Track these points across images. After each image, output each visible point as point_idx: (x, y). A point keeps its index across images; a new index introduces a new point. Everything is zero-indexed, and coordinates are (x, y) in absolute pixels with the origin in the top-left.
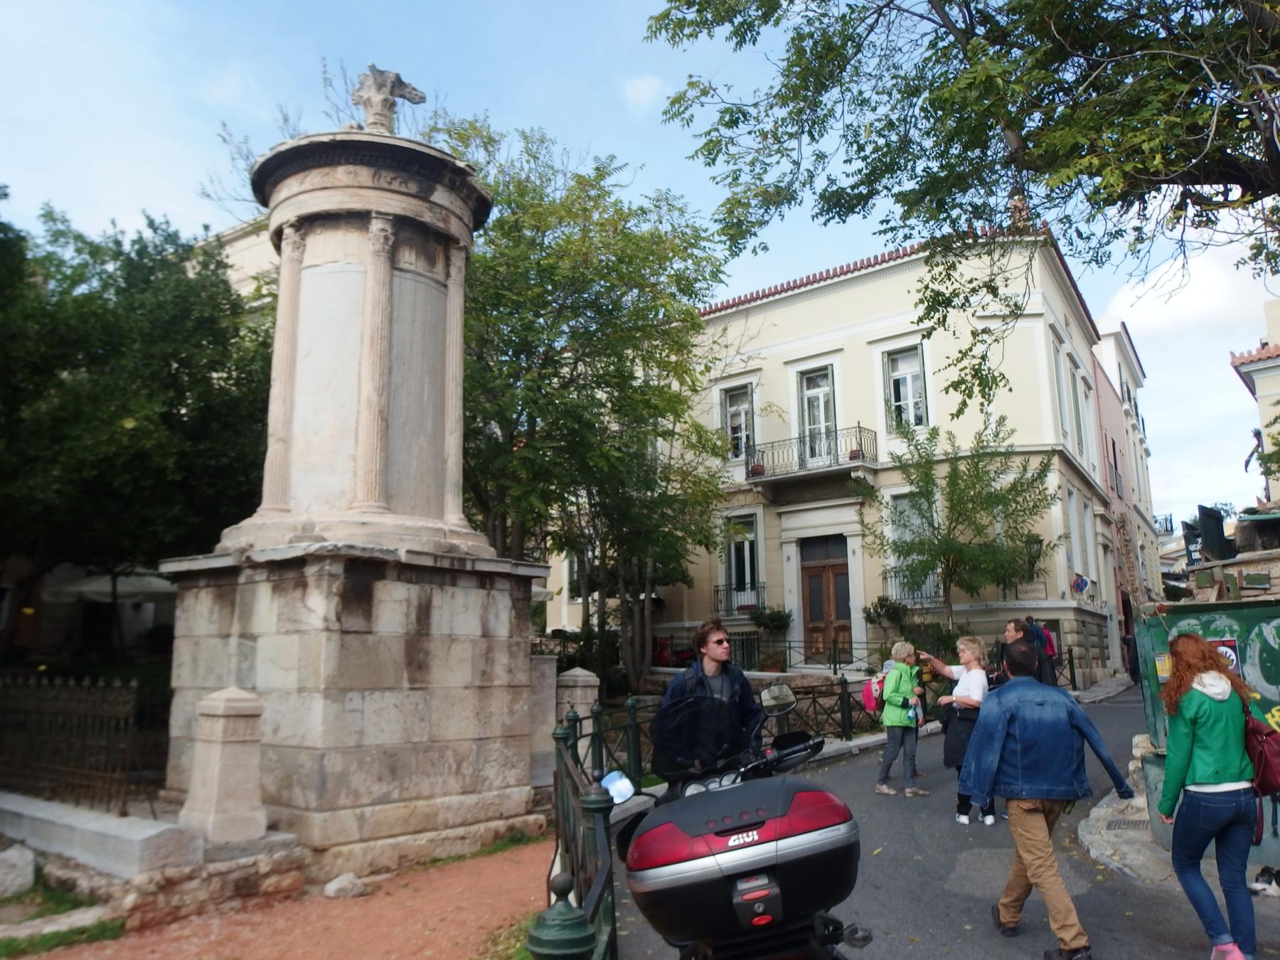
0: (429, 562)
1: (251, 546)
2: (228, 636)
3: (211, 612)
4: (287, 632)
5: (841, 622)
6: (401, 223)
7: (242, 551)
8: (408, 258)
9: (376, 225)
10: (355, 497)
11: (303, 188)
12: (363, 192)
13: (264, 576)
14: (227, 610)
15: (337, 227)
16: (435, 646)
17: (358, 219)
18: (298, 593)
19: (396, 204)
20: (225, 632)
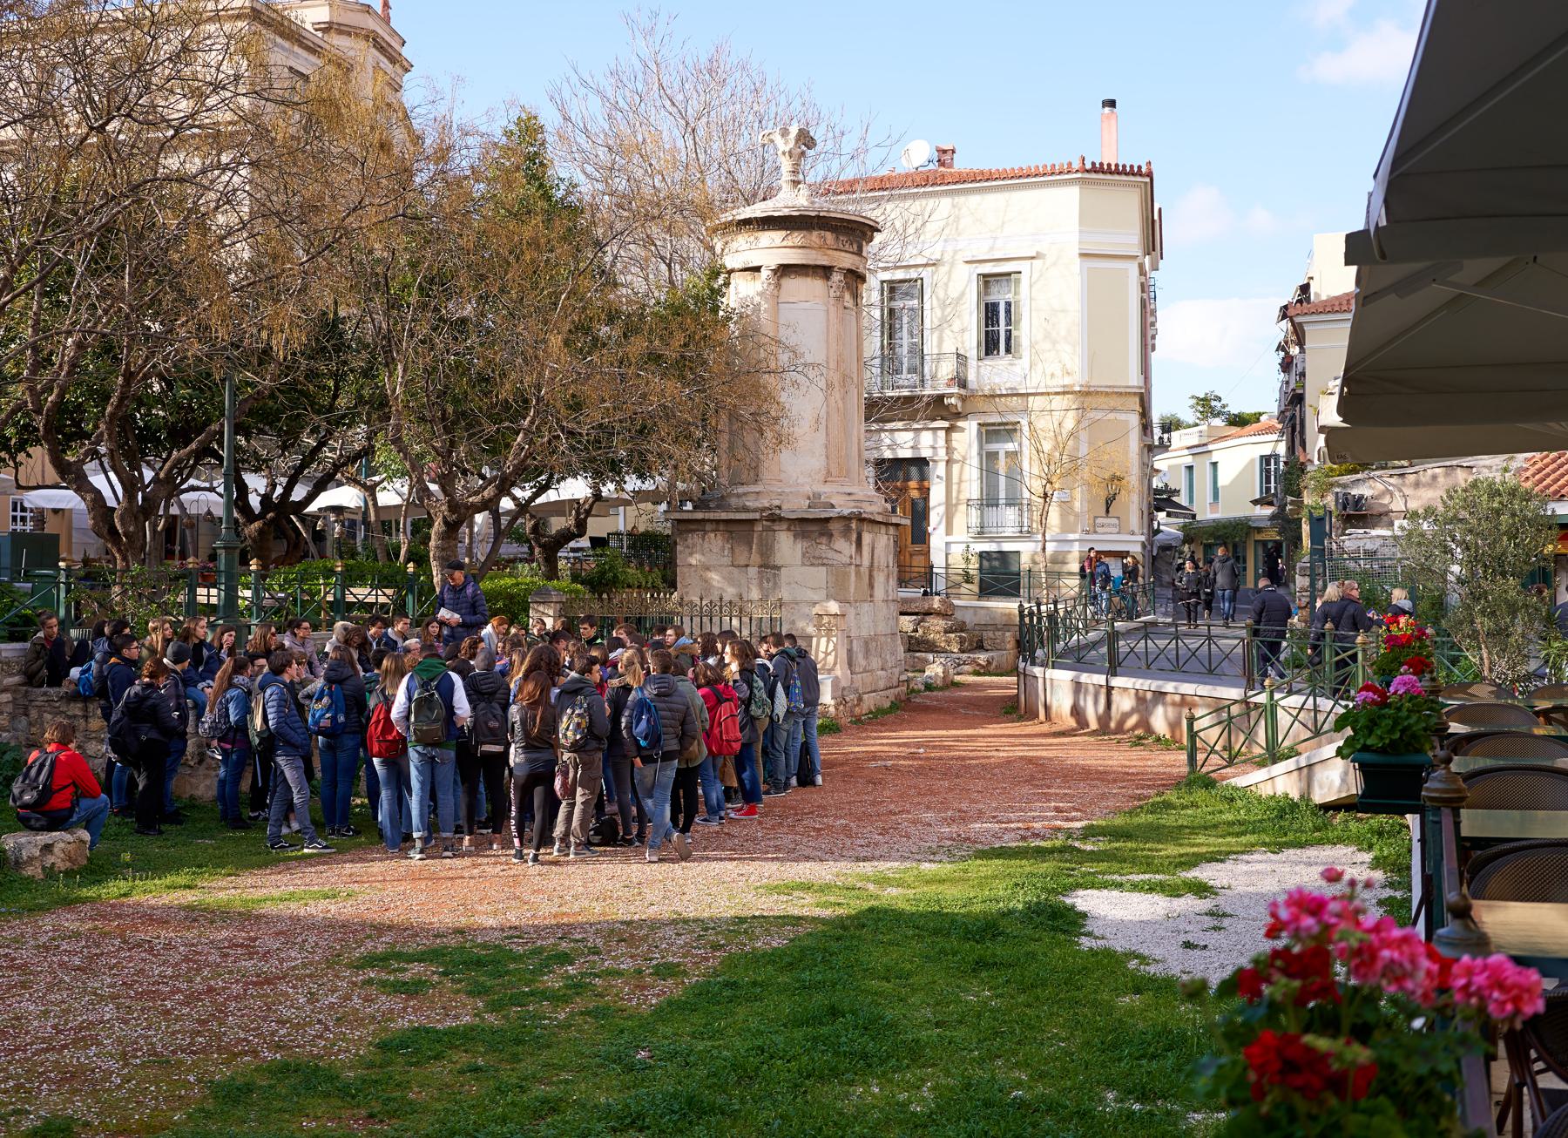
0: (879, 519)
1: (779, 508)
2: (747, 566)
3: (723, 549)
4: (812, 565)
5: (917, 548)
6: (850, 271)
7: (763, 510)
8: (847, 296)
9: (837, 277)
10: (829, 473)
11: (784, 244)
12: (830, 252)
13: (785, 526)
14: (744, 548)
15: (807, 275)
16: (875, 573)
17: (825, 271)
18: (824, 540)
19: (846, 260)
20: (743, 563)
